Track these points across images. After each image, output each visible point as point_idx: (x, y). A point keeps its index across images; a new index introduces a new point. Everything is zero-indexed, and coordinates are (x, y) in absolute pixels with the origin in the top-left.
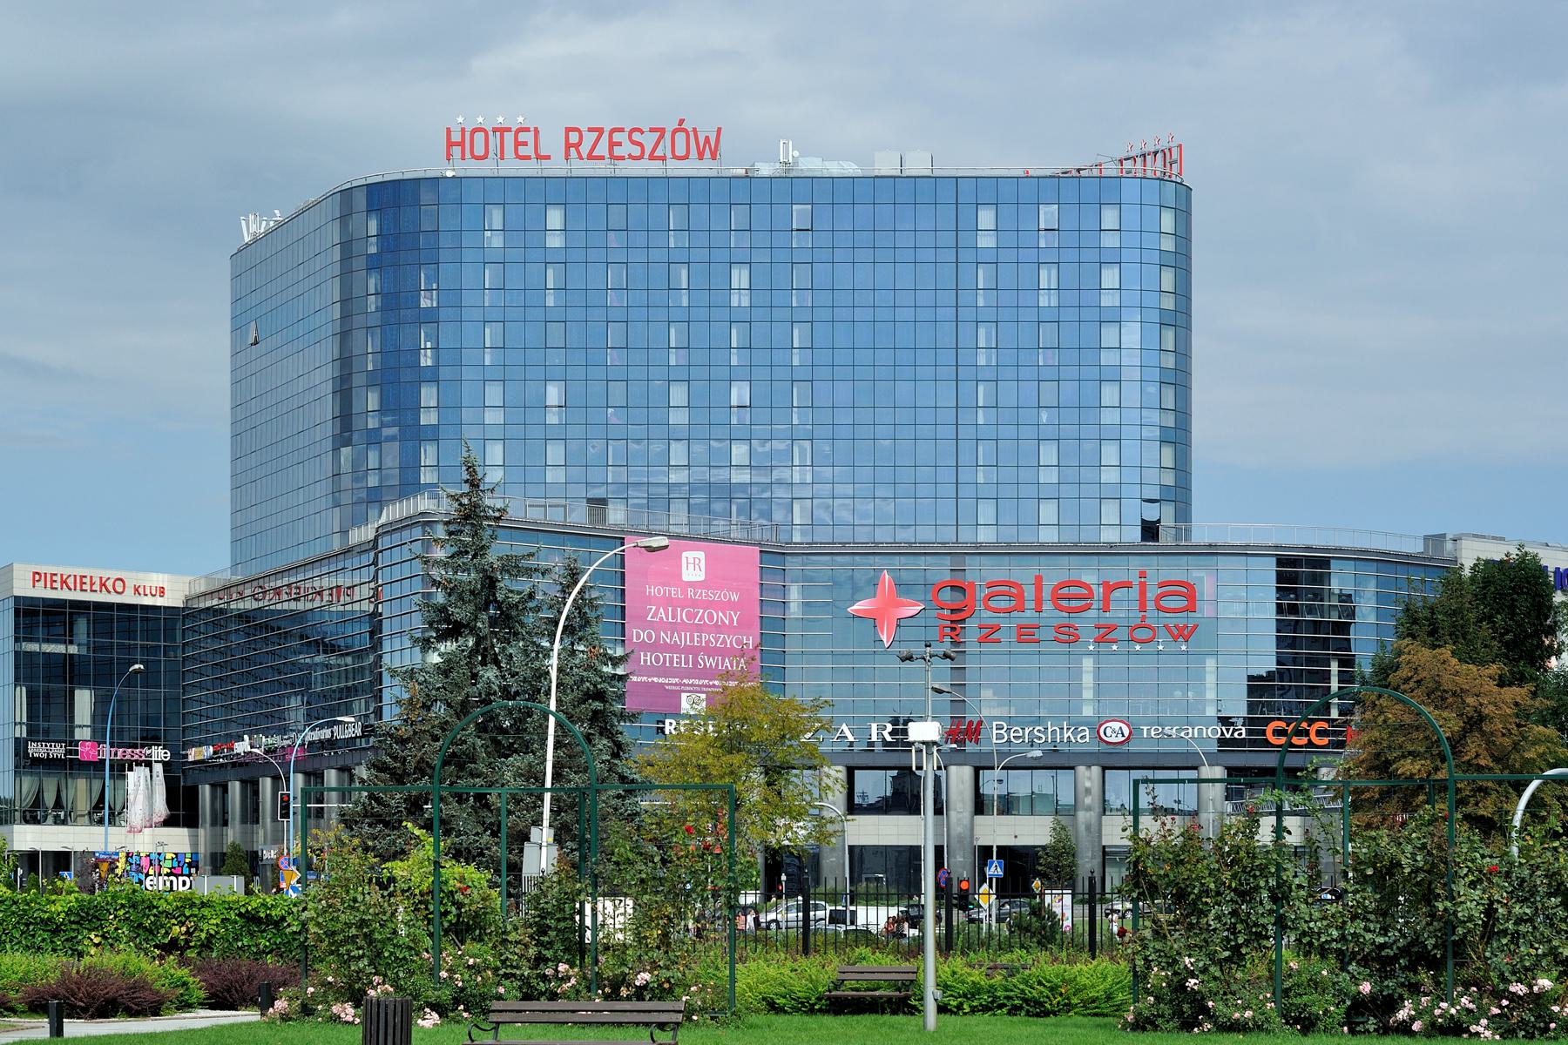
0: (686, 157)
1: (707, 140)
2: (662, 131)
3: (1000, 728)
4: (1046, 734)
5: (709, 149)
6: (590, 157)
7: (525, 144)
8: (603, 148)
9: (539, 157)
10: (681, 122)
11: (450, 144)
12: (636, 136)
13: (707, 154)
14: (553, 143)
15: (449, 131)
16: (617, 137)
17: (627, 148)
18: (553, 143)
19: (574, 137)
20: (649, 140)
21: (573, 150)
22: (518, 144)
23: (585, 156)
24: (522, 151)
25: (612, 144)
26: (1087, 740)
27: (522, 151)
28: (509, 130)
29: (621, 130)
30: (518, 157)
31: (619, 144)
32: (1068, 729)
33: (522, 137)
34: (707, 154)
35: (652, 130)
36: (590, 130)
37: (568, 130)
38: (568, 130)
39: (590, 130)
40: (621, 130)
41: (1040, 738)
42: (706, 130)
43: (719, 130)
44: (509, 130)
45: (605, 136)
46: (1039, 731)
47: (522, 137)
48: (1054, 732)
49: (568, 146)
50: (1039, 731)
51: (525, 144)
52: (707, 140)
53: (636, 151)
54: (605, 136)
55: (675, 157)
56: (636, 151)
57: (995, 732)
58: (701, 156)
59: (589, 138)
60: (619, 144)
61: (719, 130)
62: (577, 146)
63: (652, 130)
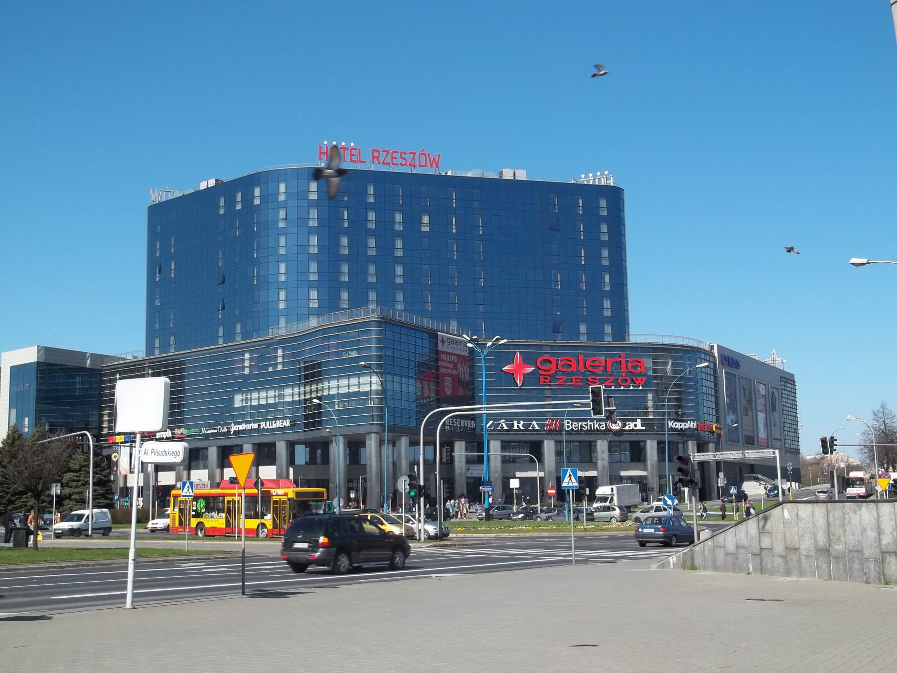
0: (425, 166)
1: (434, 159)
2: (414, 154)
4: (587, 426)
5: (435, 163)
6: (384, 163)
7: (354, 155)
8: (388, 160)
9: (361, 162)
10: (423, 150)
11: (321, 153)
12: (403, 155)
13: (434, 165)
14: (367, 156)
15: (320, 147)
17: (399, 161)
18: (367, 156)
19: (376, 154)
20: (409, 157)
21: (375, 160)
22: (351, 155)
23: (382, 163)
24: (354, 158)
25: (393, 158)
26: (604, 428)
27: (354, 158)
28: (347, 149)
29: (397, 152)
30: (352, 161)
31: (396, 158)
32: (596, 424)
33: (353, 152)
34: (434, 165)
35: (410, 153)
36: (384, 151)
37: (374, 150)
38: (374, 150)
39: (384, 151)
40: (397, 152)
41: (585, 428)
43: (439, 156)
44: (347, 149)
45: (390, 154)
46: (584, 424)
47: (353, 152)
48: (591, 425)
49: (374, 157)
50: (584, 424)
51: (354, 155)
52: (434, 159)
53: (404, 162)
54: (390, 154)
55: (420, 166)
56: (404, 162)
57: (566, 425)
58: (431, 165)
59: (383, 155)
60: (396, 158)
61: (439, 156)
62: (377, 158)
63: (410, 153)
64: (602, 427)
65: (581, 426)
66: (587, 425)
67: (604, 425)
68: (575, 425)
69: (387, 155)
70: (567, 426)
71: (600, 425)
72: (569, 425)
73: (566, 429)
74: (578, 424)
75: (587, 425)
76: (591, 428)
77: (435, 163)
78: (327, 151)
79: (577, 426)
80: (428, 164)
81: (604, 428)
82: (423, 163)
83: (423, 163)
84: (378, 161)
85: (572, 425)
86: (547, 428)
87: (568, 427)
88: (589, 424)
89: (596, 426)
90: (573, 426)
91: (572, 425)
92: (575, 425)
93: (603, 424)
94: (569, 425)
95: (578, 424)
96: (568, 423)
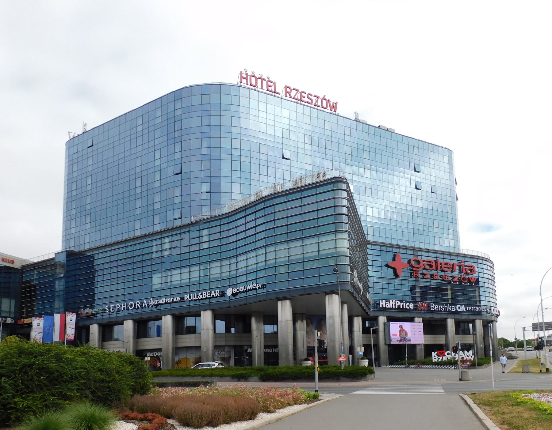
2: (318, 97)
3: (432, 305)
4: (444, 308)
7: (271, 87)
11: (242, 78)
12: (310, 96)
16: (303, 94)
19: (288, 90)
20: (314, 99)
22: (268, 86)
26: (454, 310)
27: (270, 88)
31: (304, 97)
32: (450, 307)
35: (315, 96)
39: (294, 89)
41: (443, 309)
42: (333, 101)
46: (442, 307)
49: (286, 92)
50: (442, 307)
51: (271, 87)
53: (310, 101)
56: (310, 101)
57: (431, 307)
62: (289, 93)
64: (453, 309)
65: (440, 307)
66: (444, 308)
67: (454, 308)
68: (437, 307)
70: (432, 308)
71: (451, 308)
73: (431, 310)
74: (438, 306)
75: (444, 308)
76: (446, 310)
79: (438, 308)
80: (329, 108)
81: (454, 310)
82: (325, 105)
83: (325, 105)
85: (435, 307)
86: (419, 309)
87: (433, 308)
88: (445, 307)
89: (450, 308)
90: (436, 308)
91: (435, 307)
92: (437, 307)
93: (453, 307)
94: (433, 307)
95: (438, 306)
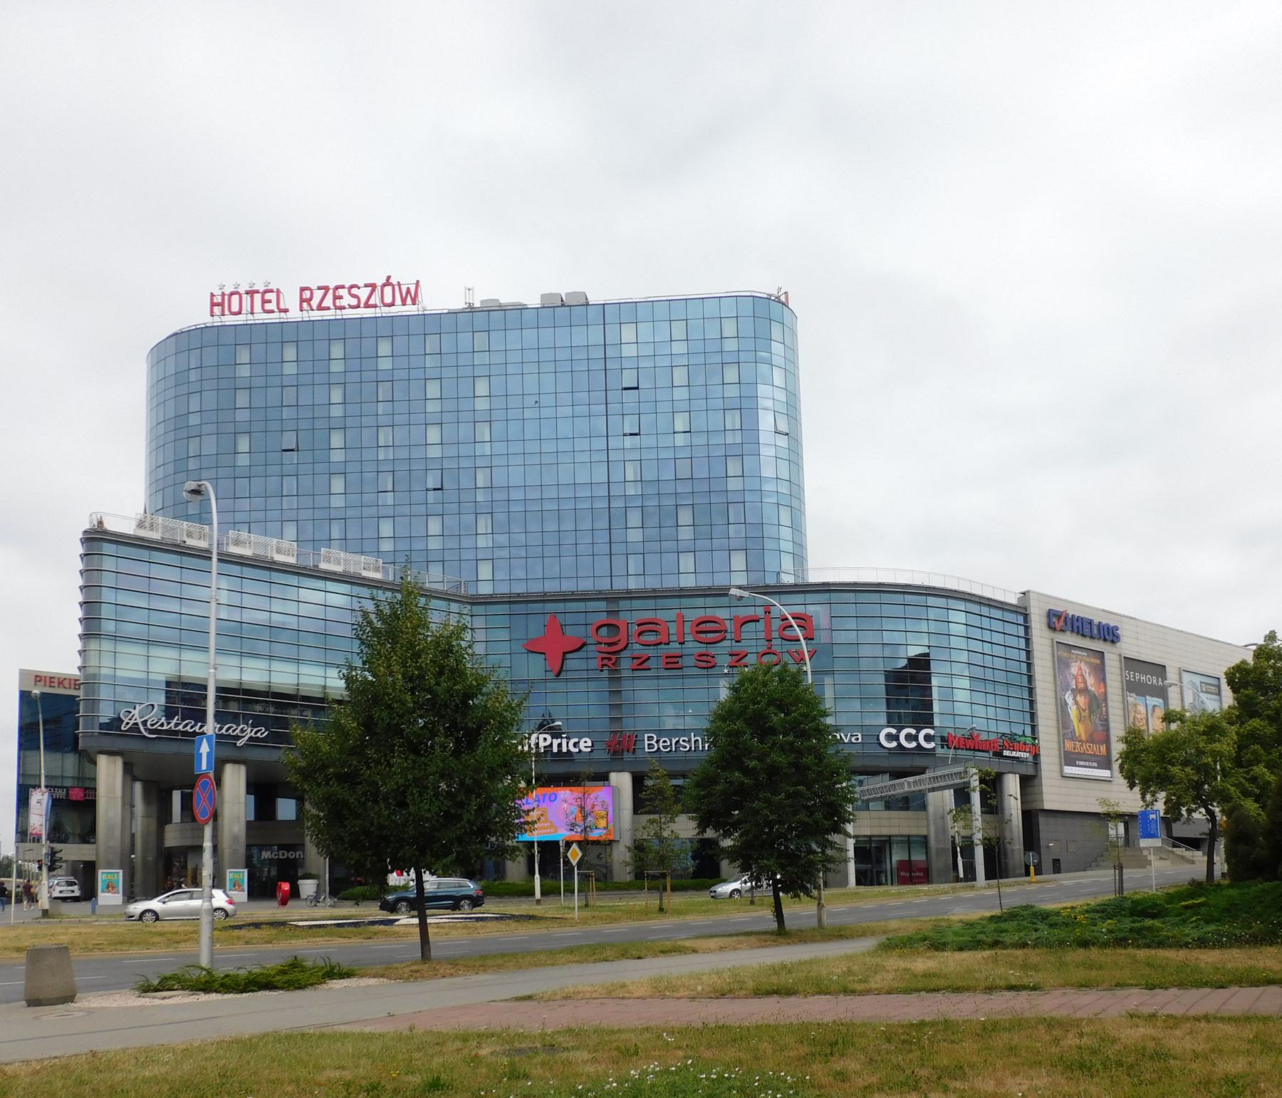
0: (392, 304)
1: (408, 291)
7: (270, 301)
8: (328, 302)
11: (213, 305)
12: (354, 291)
13: (409, 301)
14: (291, 301)
15: (212, 295)
17: (347, 300)
18: (291, 301)
21: (305, 305)
22: (264, 302)
24: (268, 306)
27: (268, 306)
29: (343, 287)
31: (341, 297)
33: (268, 296)
34: (409, 301)
35: (366, 286)
36: (319, 288)
37: (303, 289)
38: (303, 289)
40: (343, 287)
45: (331, 292)
46: (684, 741)
47: (268, 296)
49: (302, 300)
51: (270, 301)
52: (408, 291)
57: (646, 742)
59: (318, 295)
63: (366, 286)
69: (114, 515)
70: (649, 745)
72: (653, 742)
75: (689, 741)
77: (412, 296)
78: (223, 299)
79: (669, 744)
80: (398, 301)
84: (310, 305)
85: (658, 742)
90: (661, 744)
91: (658, 742)
92: (665, 742)
94: (653, 742)
95: (671, 741)
96: (650, 738)
